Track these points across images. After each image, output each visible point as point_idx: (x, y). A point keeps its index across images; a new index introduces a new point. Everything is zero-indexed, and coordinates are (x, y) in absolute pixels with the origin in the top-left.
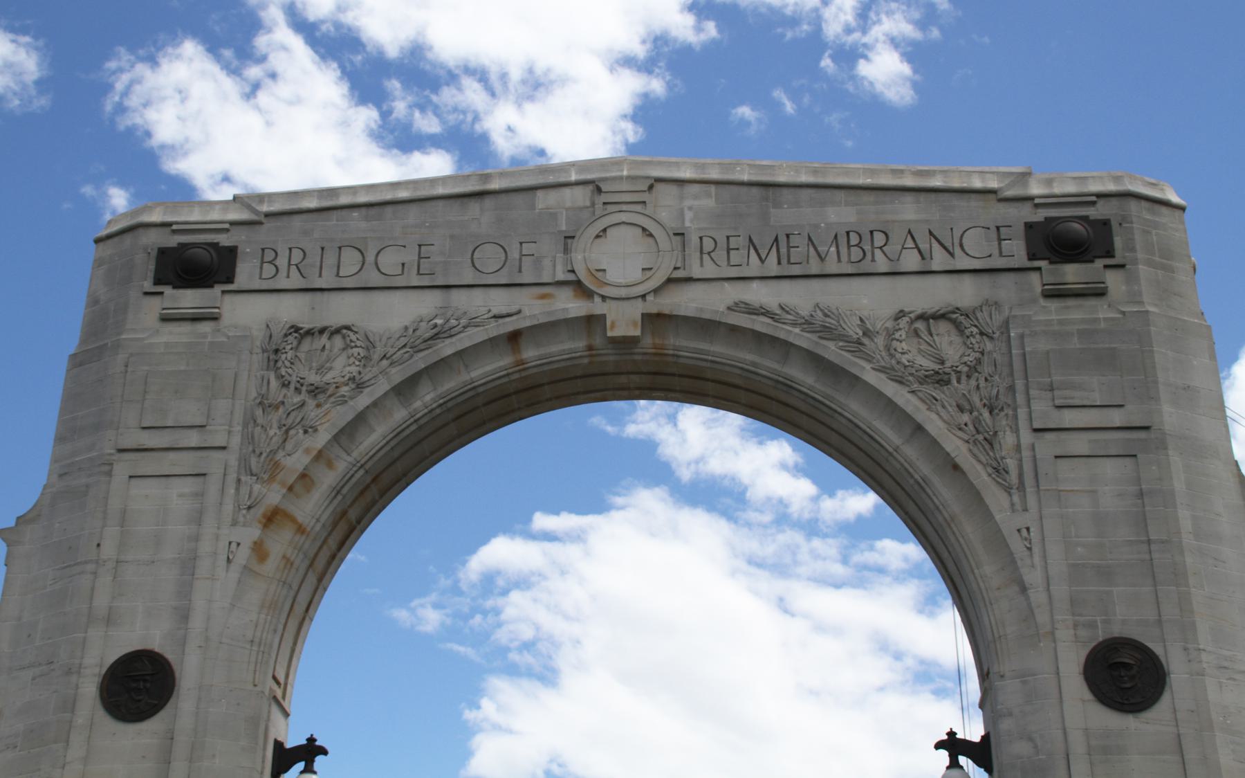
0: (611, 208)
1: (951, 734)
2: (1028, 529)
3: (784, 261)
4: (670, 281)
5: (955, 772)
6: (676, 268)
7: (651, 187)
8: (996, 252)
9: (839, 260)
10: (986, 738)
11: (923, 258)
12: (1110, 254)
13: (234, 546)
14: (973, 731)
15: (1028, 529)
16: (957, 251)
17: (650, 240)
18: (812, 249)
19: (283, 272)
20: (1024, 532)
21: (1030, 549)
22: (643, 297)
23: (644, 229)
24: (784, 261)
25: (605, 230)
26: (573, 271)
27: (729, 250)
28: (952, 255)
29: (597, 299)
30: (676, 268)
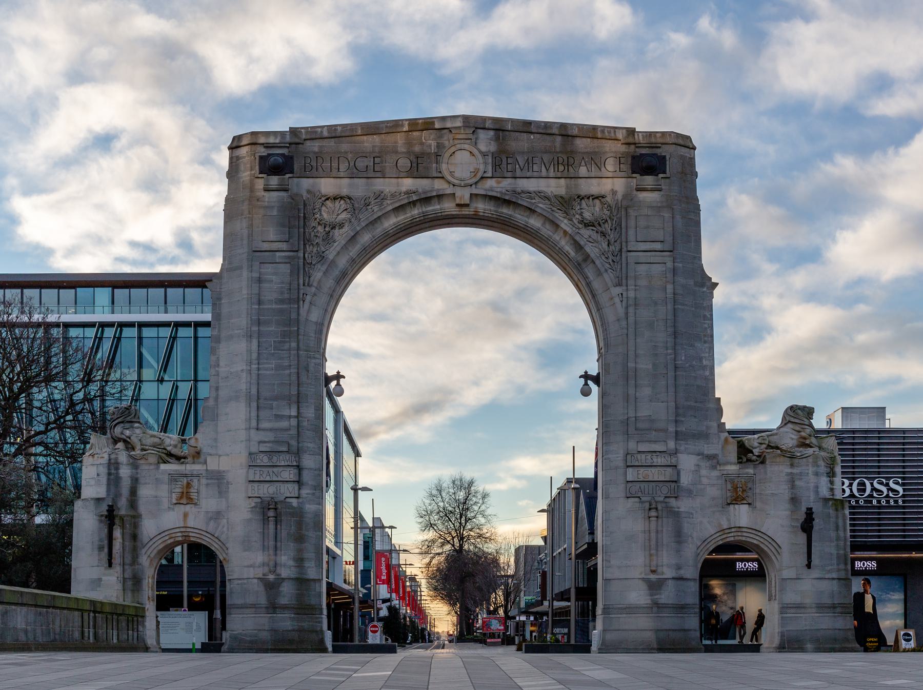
0: (456, 142)
1: (586, 372)
2: (622, 294)
3: (531, 170)
4: (482, 178)
5: (586, 386)
6: (485, 172)
7: (474, 132)
8: (618, 170)
9: (554, 171)
10: (599, 374)
11: (588, 171)
12: (664, 172)
13: (305, 295)
14: (594, 371)
15: (622, 294)
16: (603, 169)
17: (473, 157)
18: (543, 165)
19: (314, 169)
20: (620, 295)
21: (622, 301)
22: (471, 185)
23: (471, 152)
24: (531, 170)
25: (454, 153)
26: (440, 172)
27: (507, 164)
28: (600, 169)
29: (452, 186)
30: (485, 172)
